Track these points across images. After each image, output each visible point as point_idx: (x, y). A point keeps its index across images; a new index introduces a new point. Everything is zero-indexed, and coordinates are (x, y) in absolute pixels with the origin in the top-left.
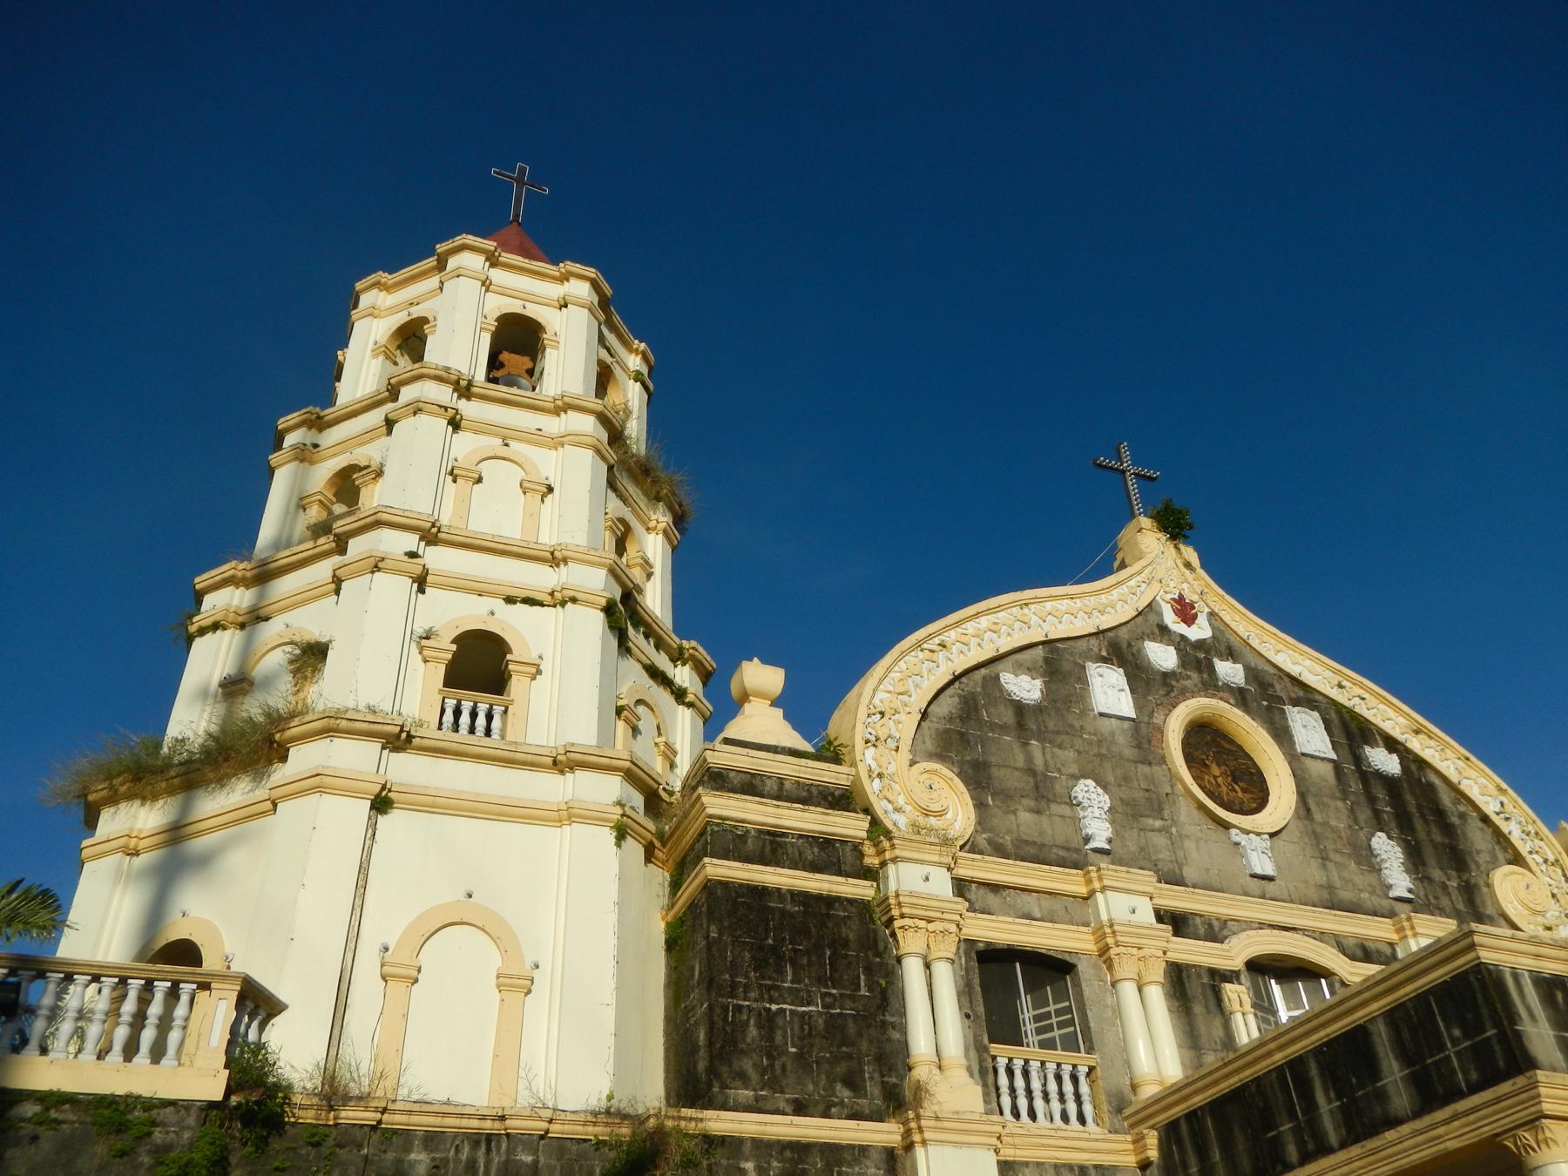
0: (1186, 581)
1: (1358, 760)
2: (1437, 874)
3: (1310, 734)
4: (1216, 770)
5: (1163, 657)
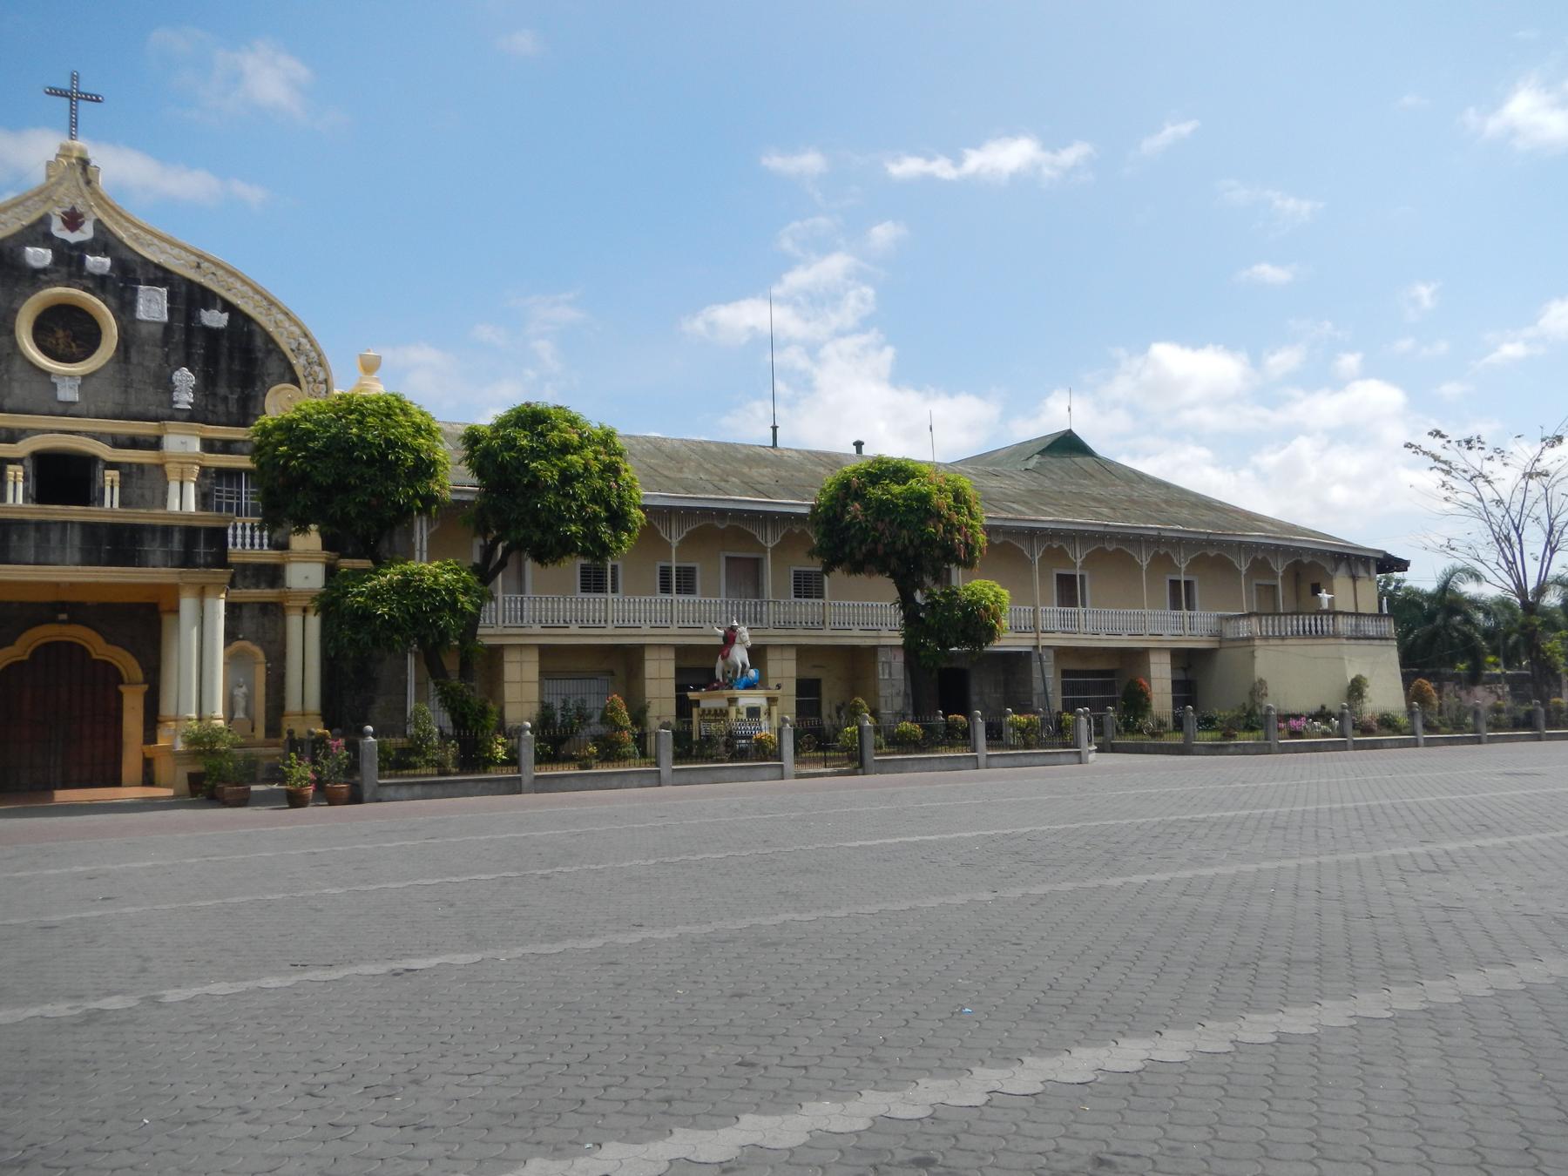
0: (82, 196)
1: (191, 317)
2: (222, 390)
3: (152, 306)
4: (60, 334)
5: (39, 256)
